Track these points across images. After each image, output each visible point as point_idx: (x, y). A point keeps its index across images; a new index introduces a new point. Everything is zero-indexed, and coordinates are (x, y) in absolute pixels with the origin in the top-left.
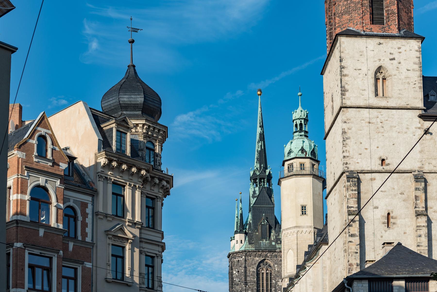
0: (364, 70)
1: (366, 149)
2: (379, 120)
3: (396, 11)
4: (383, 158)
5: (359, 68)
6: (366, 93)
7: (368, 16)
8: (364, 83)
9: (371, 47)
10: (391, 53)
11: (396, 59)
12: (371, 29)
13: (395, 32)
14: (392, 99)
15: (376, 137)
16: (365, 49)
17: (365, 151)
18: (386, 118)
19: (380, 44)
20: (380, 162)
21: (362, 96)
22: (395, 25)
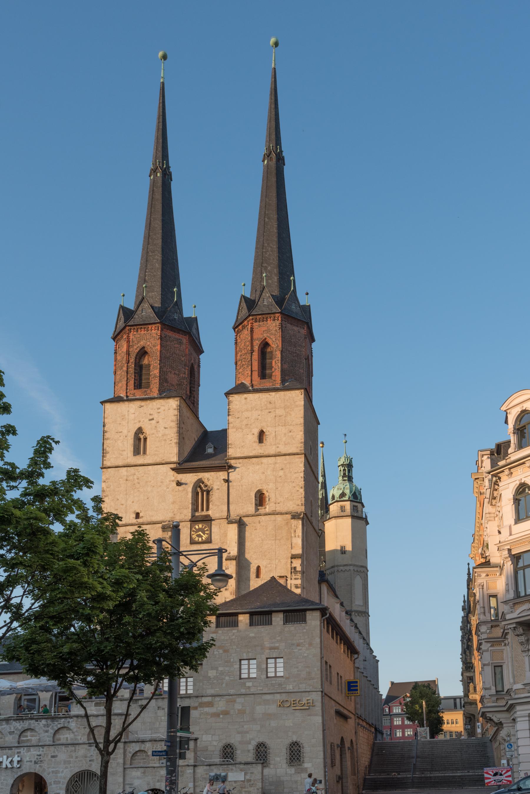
0: (125, 432)
1: (122, 504)
2: (135, 477)
3: (158, 375)
4: (137, 511)
5: (120, 431)
6: (125, 453)
7: (132, 382)
8: (123, 444)
9: (132, 411)
10: (150, 414)
11: (155, 419)
12: (135, 393)
13: (155, 393)
14: (149, 457)
15: (132, 492)
16: (126, 413)
17: (121, 506)
18: (142, 475)
19: (142, 406)
20: (134, 516)
21: (122, 457)
22: (157, 387)
